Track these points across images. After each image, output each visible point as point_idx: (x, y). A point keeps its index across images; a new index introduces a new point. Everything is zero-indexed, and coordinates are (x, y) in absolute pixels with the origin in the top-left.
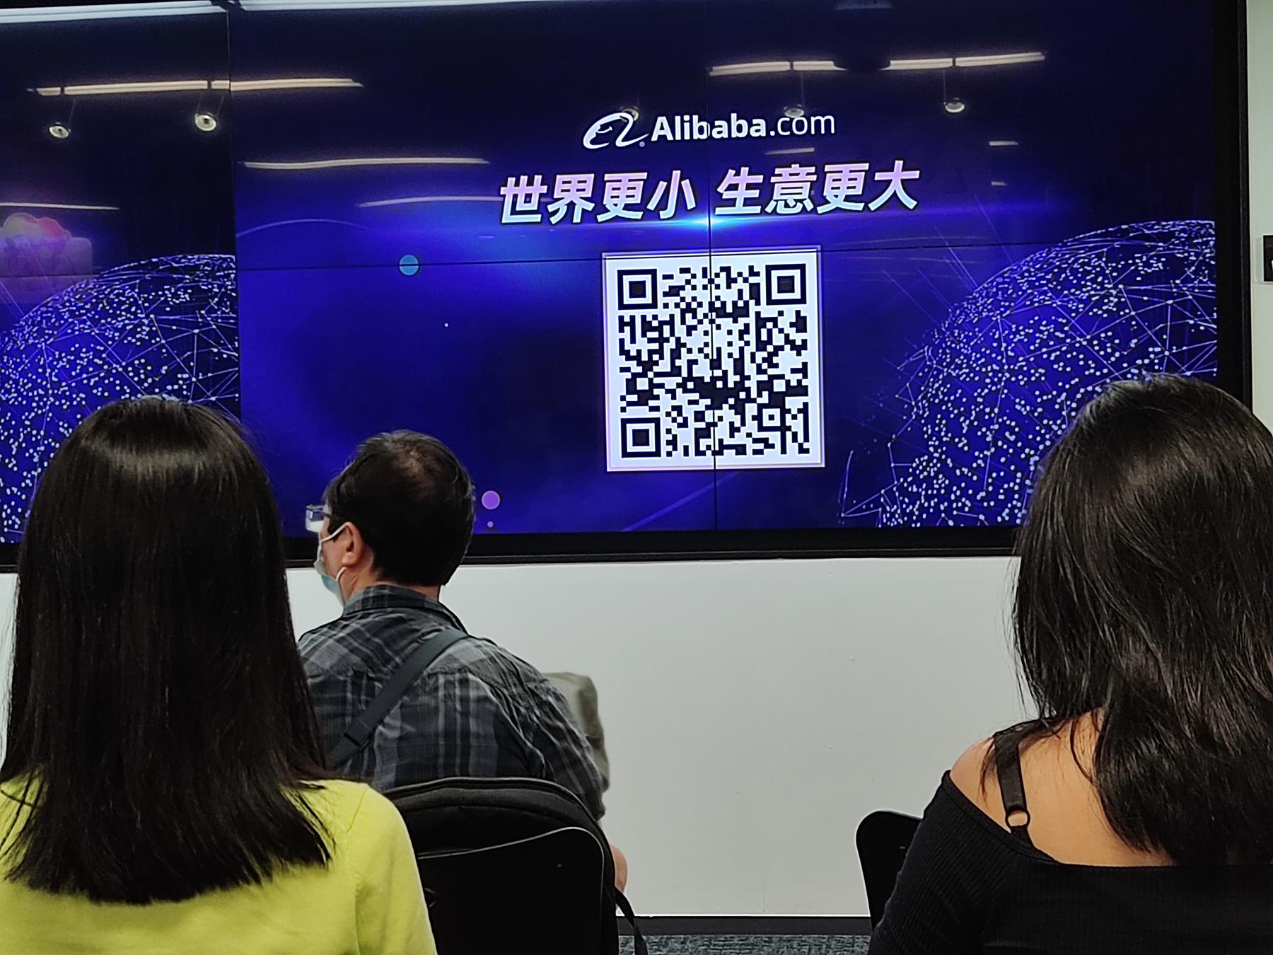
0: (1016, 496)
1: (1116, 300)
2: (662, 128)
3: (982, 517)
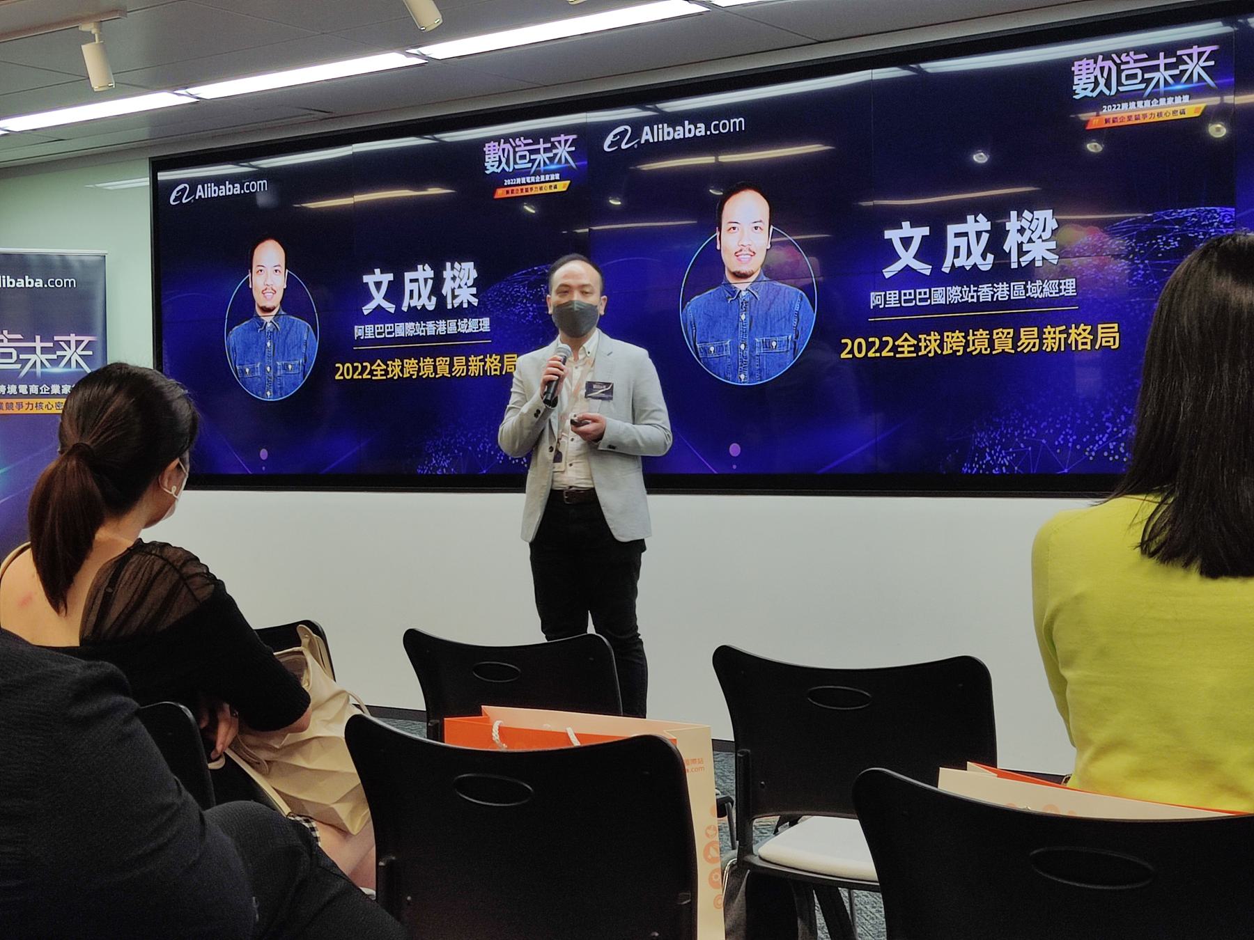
0: (1069, 426)
1: (1143, 272)
2: (647, 134)
3: (1044, 441)
